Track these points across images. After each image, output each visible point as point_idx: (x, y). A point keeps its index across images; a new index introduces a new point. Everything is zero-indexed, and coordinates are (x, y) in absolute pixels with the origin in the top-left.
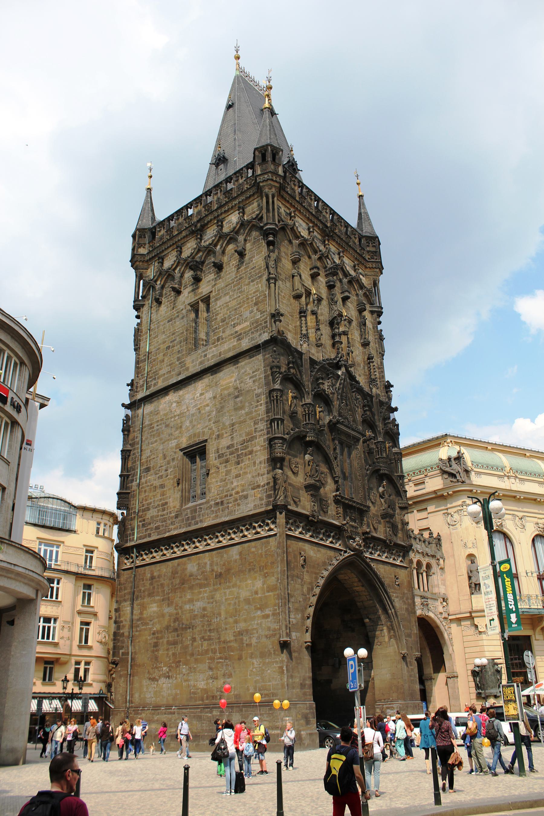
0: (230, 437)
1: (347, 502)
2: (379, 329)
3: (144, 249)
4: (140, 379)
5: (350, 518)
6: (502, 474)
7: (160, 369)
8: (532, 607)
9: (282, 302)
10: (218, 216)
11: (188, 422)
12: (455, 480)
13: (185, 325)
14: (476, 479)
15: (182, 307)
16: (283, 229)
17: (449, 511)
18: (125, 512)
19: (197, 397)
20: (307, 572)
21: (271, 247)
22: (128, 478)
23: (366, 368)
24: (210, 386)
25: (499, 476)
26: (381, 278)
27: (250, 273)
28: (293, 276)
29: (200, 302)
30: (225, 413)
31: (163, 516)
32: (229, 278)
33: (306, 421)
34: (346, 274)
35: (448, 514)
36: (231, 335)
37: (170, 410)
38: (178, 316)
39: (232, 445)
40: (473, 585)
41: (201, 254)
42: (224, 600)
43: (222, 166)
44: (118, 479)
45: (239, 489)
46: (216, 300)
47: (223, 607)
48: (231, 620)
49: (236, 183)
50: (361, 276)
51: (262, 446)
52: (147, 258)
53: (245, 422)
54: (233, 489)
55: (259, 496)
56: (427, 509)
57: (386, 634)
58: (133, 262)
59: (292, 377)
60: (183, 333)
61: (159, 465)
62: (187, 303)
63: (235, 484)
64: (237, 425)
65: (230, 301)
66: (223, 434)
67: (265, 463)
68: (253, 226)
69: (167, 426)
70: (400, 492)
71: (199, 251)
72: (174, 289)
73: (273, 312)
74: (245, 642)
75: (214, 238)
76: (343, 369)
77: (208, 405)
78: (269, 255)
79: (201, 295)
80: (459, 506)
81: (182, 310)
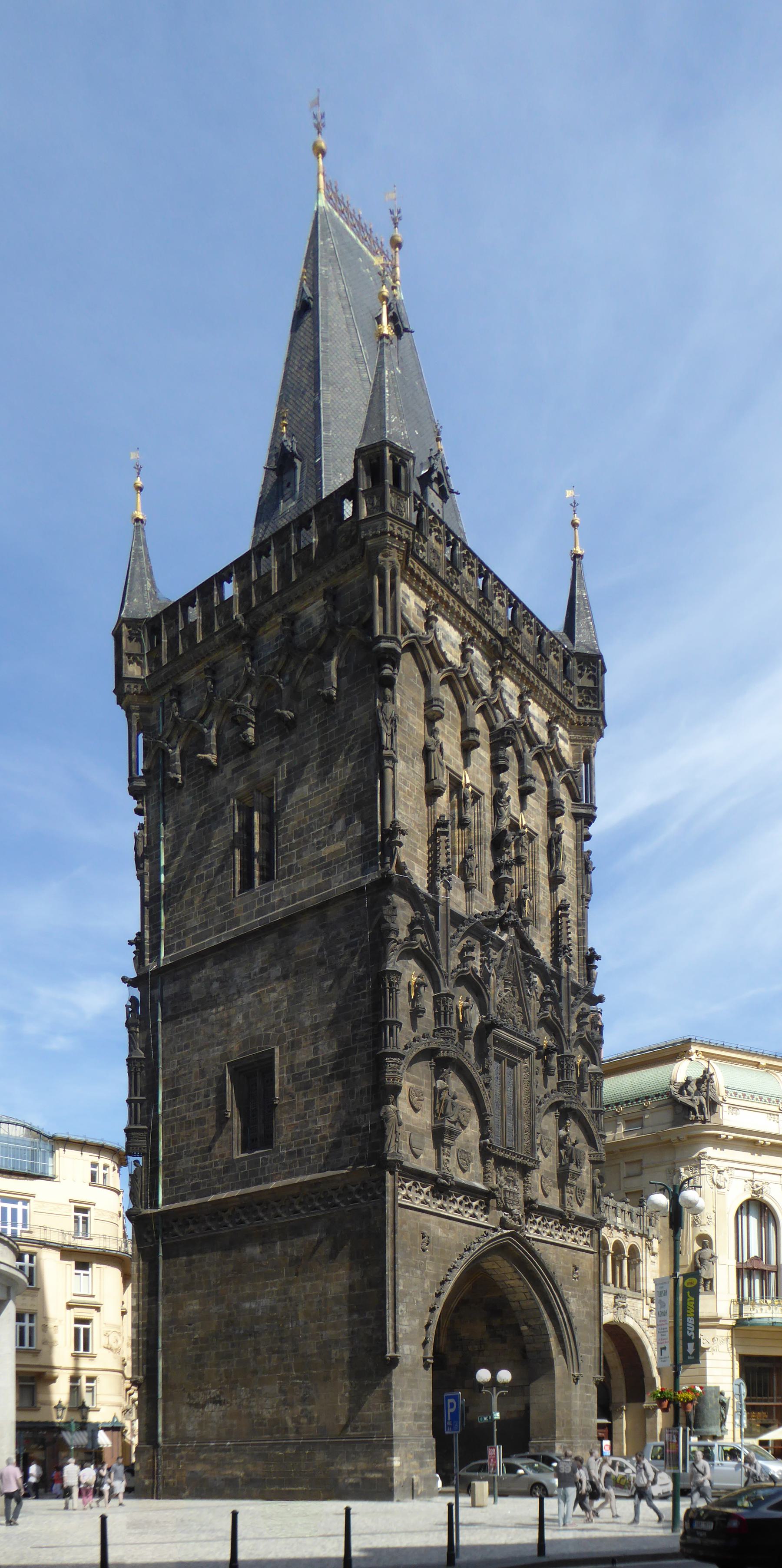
1: (501, 1154)
9: (405, 804)
18: (140, 1159)
20: (432, 1259)
33: (440, 1024)
42: (303, 1297)
44: (126, 1107)
47: (300, 1307)
48: (312, 1325)
54: (317, 1132)
55: (359, 1144)
61: (194, 1086)
63: (320, 1124)
66: (299, 1041)
74: (333, 1356)
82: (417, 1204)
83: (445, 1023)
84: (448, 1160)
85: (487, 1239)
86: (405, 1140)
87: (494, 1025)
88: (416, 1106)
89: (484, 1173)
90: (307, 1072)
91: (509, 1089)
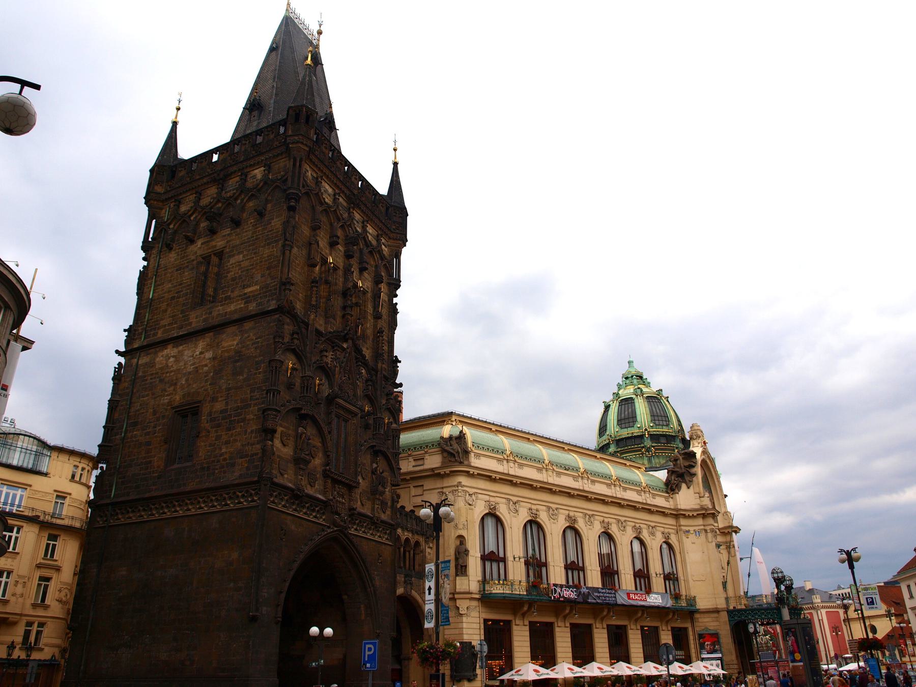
0: (225, 401)
2: (394, 302)
3: (161, 187)
4: (139, 326)
5: (338, 493)
6: (502, 457)
7: (162, 319)
8: (514, 592)
9: (295, 270)
10: (243, 168)
11: (184, 380)
12: (453, 459)
13: (193, 277)
14: (475, 461)
15: (193, 257)
16: (307, 194)
17: (445, 490)
19: (196, 356)
21: (292, 213)
22: (112, 429)
23: (375, 341)
24: (210, 346)
25: (499, 460)
26: (404, 250)
27: (268, 235)
28: (311, 244)
29: (212, 256)
30: (223, 376)
31: (145, 475)
32: (245, 237)
33: (304, 393)
34: (367, 244)
35: (443, 493)
36: (240, 296)
37: (166, 364)
38: (187, 267)
39: (226, 410)
40: (459, 567)
41: (220, 205)
43: (256, 113)
45: (227, 456)
46: (230, 257)
49: (266, 137)
50: (383, 246)
51: (256, 415)
52: (164, 197)
53: (241, 388)
54: (221, 455)
55: (246, 465)
56: (423, 485)
57: (363, 612)
58: (148, 200)
59: (295, 348)
60: (191, 285)
62: (199, 253)
64: (233, 390)
65: (243, 261)
67: (256, 433)
68: (277, 187)
69: (161, 381)
70: (394, 468)
71: (218, 201)
72: (187, 237)
73: (284, 280)
75: (235, 191)
76: (350, 342)
77: (206, 365)
78: (288, 221)
79: (215, 249)
80: (454, 486)
81: (193, 260)
82: (280, 507)
83: (307, 393)
84: (302, 479)
85: (323, 534)
86: (276, 464)
87: (337, 396)
88: (285, 443)
89: (325, 489)
90: (220, 417)
91: (343, 436)
